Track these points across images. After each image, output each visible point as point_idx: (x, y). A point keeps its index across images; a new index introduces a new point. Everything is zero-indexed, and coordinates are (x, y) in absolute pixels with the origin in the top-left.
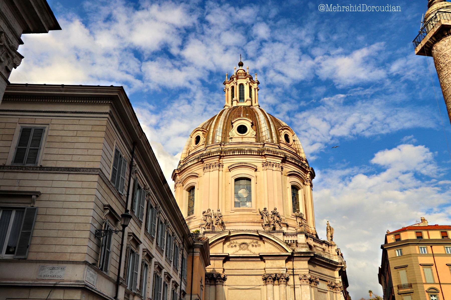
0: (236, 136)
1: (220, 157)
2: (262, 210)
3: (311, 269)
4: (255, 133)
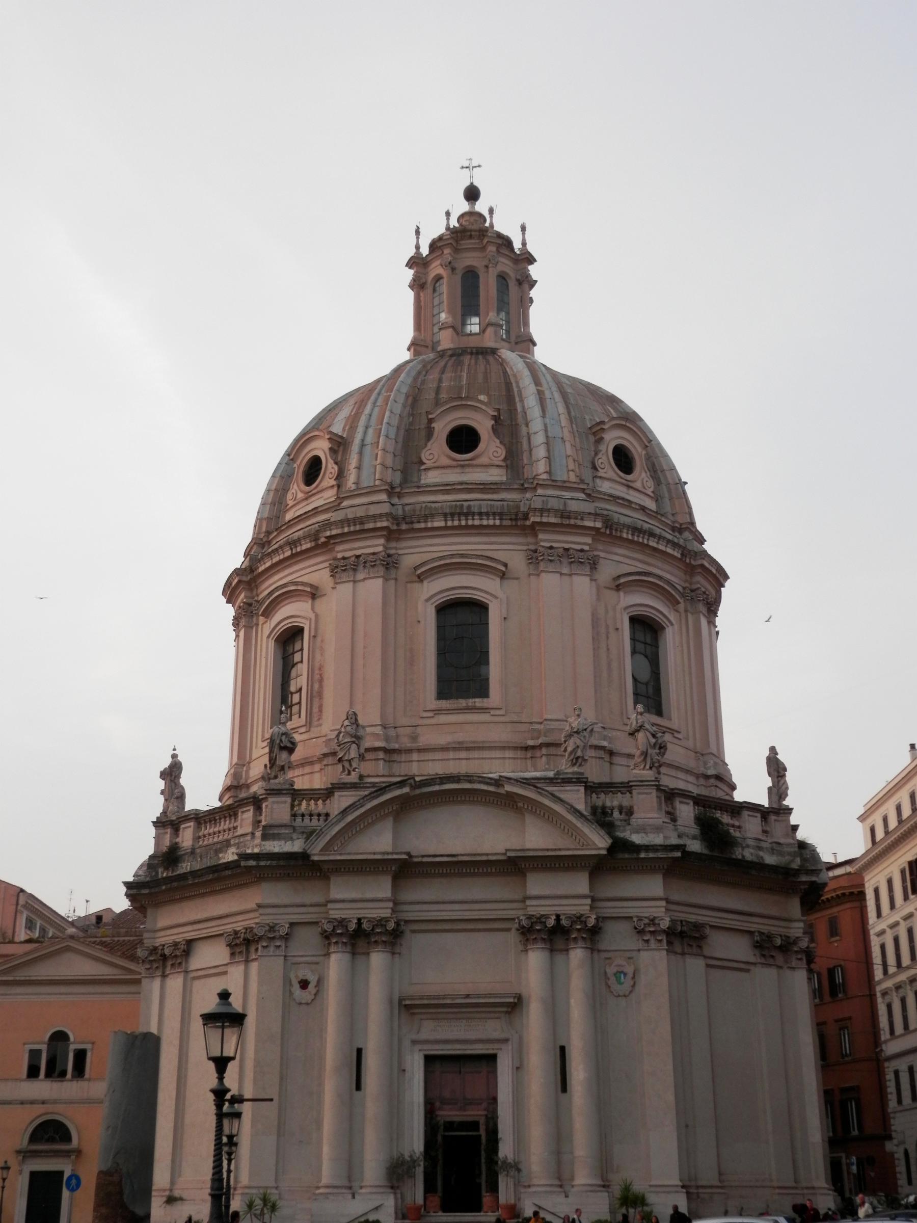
1: (391, 535)
3: (675, 897)
4: (502, 452)
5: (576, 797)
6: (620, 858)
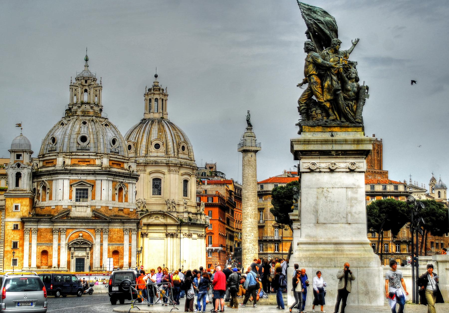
0: (154, 151)
1: (145, 166)
2: (167, 199)
5: (175, 215)
6: (181, 224)
